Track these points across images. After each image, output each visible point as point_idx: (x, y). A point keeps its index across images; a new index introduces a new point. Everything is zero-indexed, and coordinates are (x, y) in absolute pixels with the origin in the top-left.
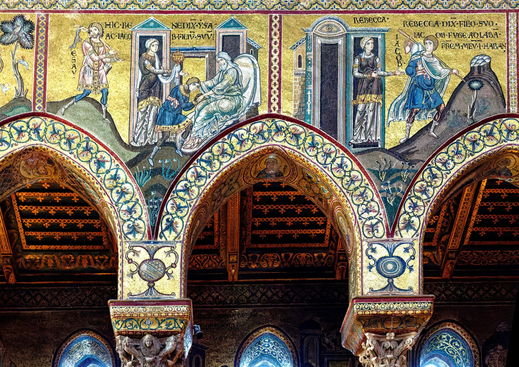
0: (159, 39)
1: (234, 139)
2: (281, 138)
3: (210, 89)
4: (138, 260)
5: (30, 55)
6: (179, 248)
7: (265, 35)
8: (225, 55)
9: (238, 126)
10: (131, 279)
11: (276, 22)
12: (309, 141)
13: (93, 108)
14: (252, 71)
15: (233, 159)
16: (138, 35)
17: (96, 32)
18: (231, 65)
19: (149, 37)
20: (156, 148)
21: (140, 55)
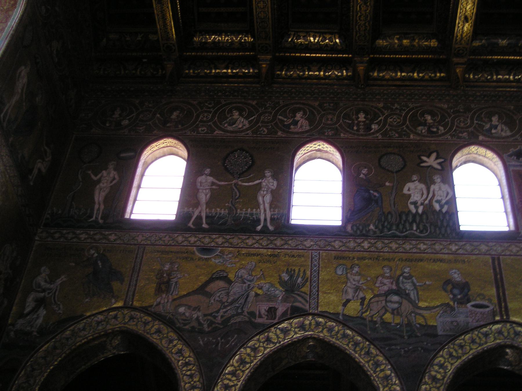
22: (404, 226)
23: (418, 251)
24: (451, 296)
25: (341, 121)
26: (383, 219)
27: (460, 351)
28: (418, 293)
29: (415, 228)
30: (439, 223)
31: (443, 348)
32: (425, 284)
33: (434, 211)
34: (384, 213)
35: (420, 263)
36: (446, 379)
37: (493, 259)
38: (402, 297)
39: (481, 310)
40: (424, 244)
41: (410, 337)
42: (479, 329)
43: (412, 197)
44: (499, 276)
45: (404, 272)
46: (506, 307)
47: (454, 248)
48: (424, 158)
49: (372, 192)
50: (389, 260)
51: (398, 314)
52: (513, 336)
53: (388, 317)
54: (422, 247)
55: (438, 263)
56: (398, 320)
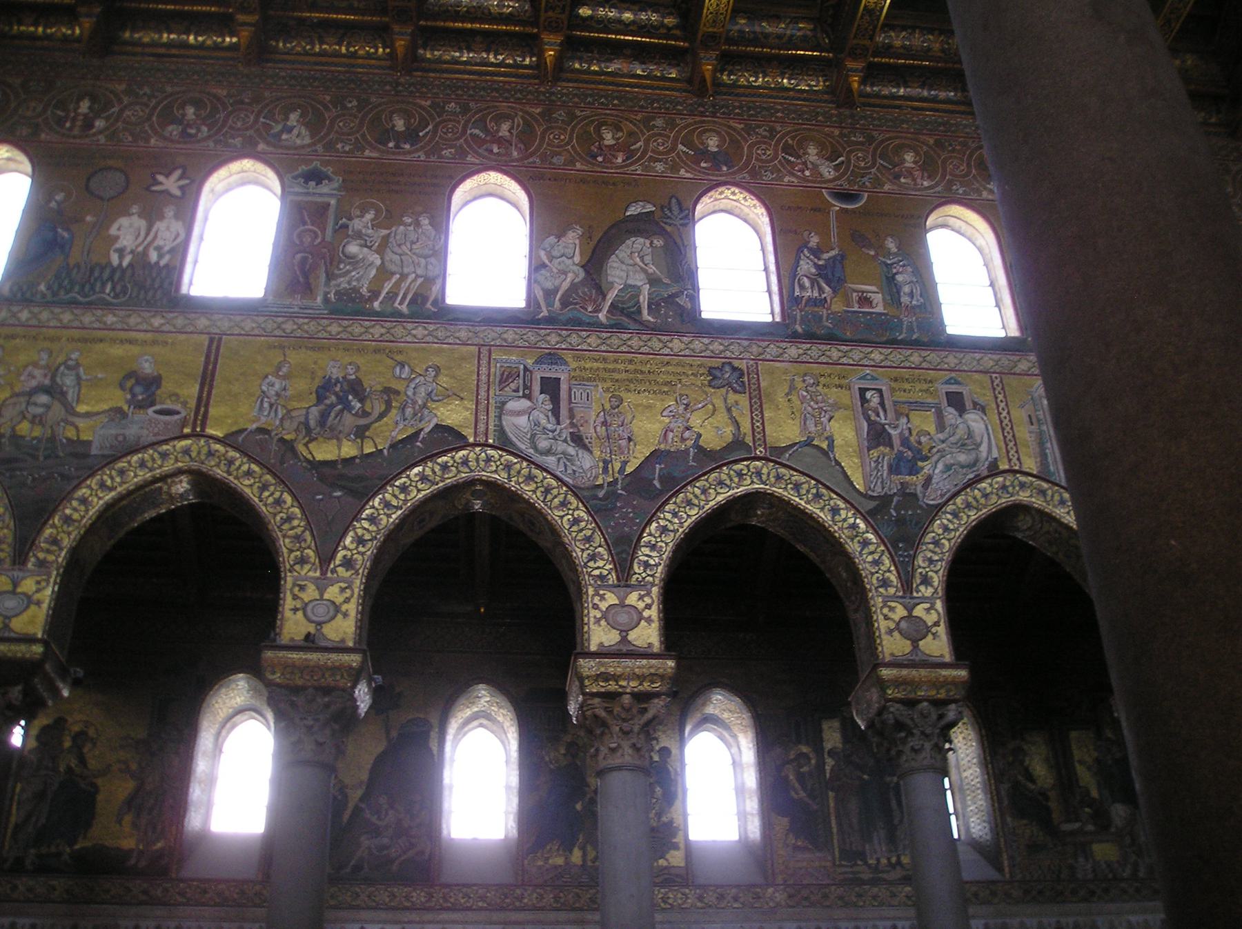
0: (880, 391)
1: (976, 491)
2: (1028, 493)
3: (943, 442)
4: (896, 617)
5: (744, 400)
6: (939, 605)
7: (989, 394)
8: (951, 410)
9: (979, 479)
10: (892, 639)
11: (997, 382)
12: (1057, 497)
13: (819, 455)
14: (983, 426)
15: (980, 513)
16: (857, 387)
17: (812, 381)
18: (959, 420)
19: (868, 389)
20: (895, 499)
21: (862, 406)
22: (92, 288)
23: (102, 326)
24: (129, 396)
25: (49, 112)
26: (64, 275)
27: (118, 479)
28: (79, 391)
29: (108, 291)
30: (149, 282)
31: (92, 475)
32: (96, 377)
33: (147, 265)
34: (68, 265)
35: (100, 347)
36: (85, 520)
37: (211, 341)
38: (53, 397)
39: (167, 418)
40: (115, 315)
41: (46, 458)
42: (156, 447)
43: (120, 241)
44: (210, 367)
45: (71, 359)
46: (206, 412)
47: (157, 322)
48: (160, 178)
49: (59, 230)
50: (52, 339)
51: (41, 423)
52: (203, 457)
53: (24, 428)
54: (110, 319)
55: (127, 346)
56: (37, 432)
